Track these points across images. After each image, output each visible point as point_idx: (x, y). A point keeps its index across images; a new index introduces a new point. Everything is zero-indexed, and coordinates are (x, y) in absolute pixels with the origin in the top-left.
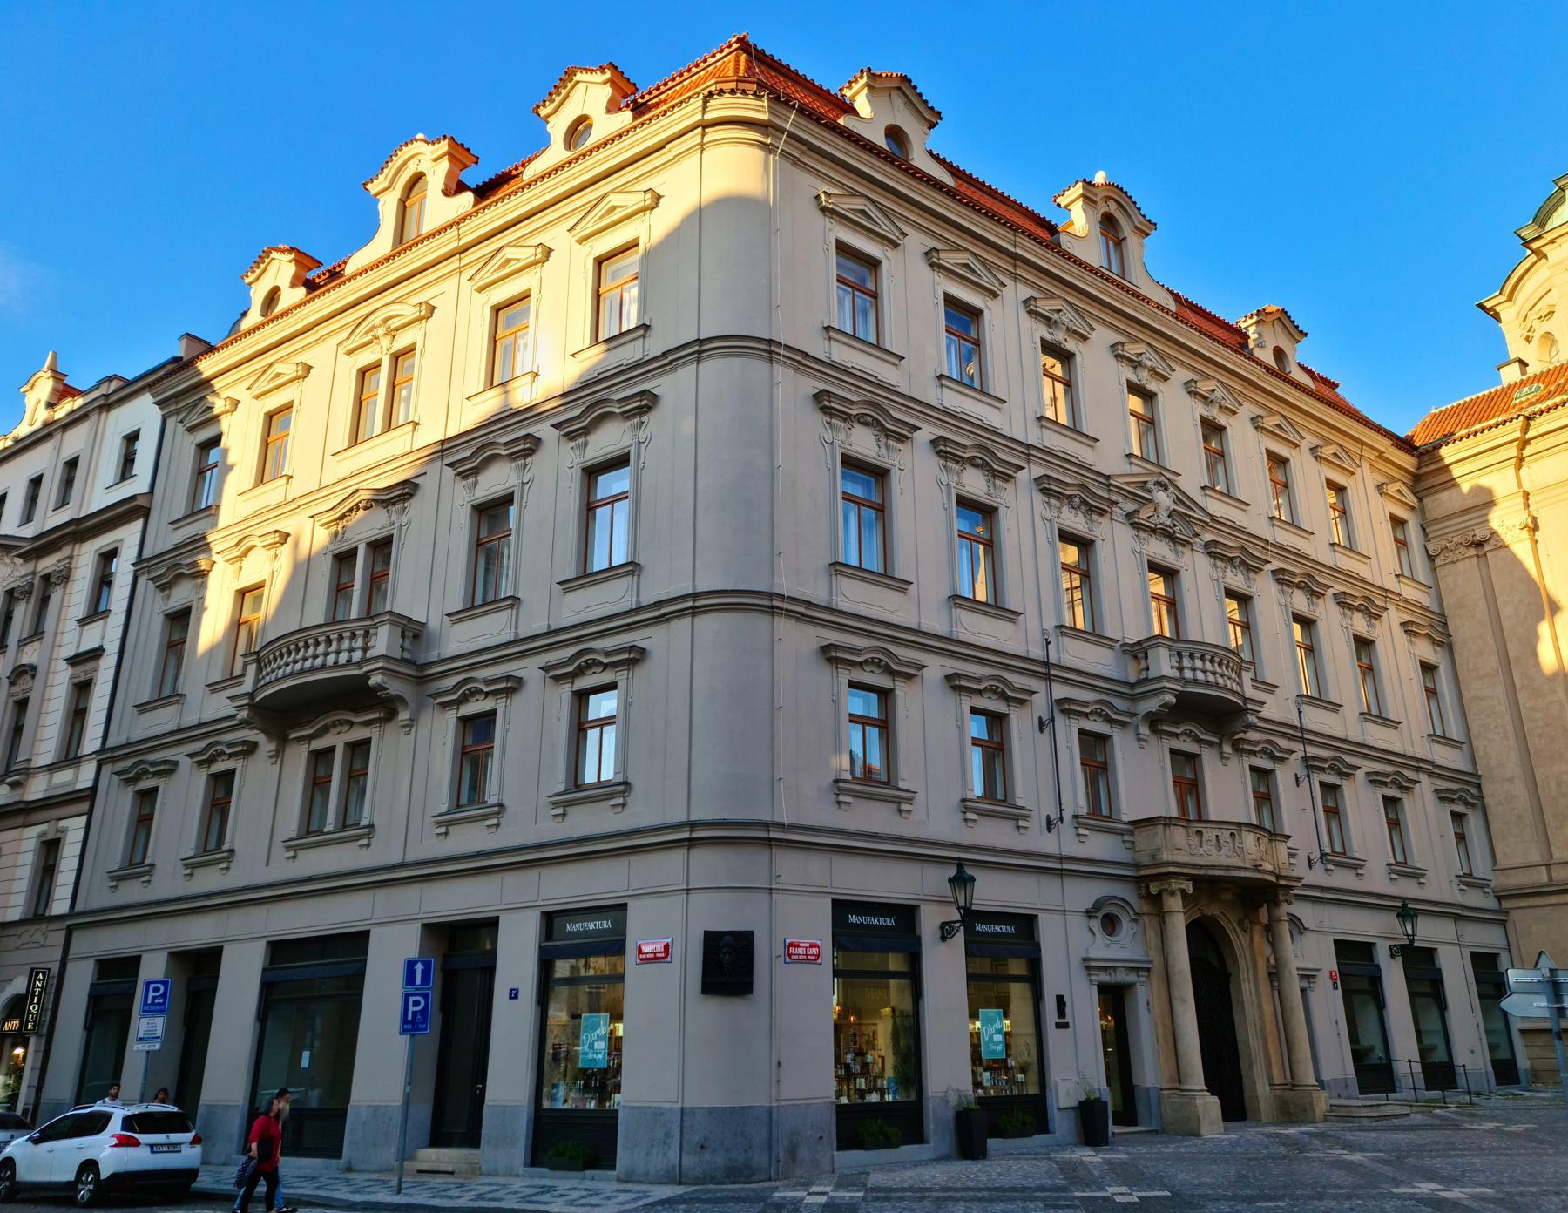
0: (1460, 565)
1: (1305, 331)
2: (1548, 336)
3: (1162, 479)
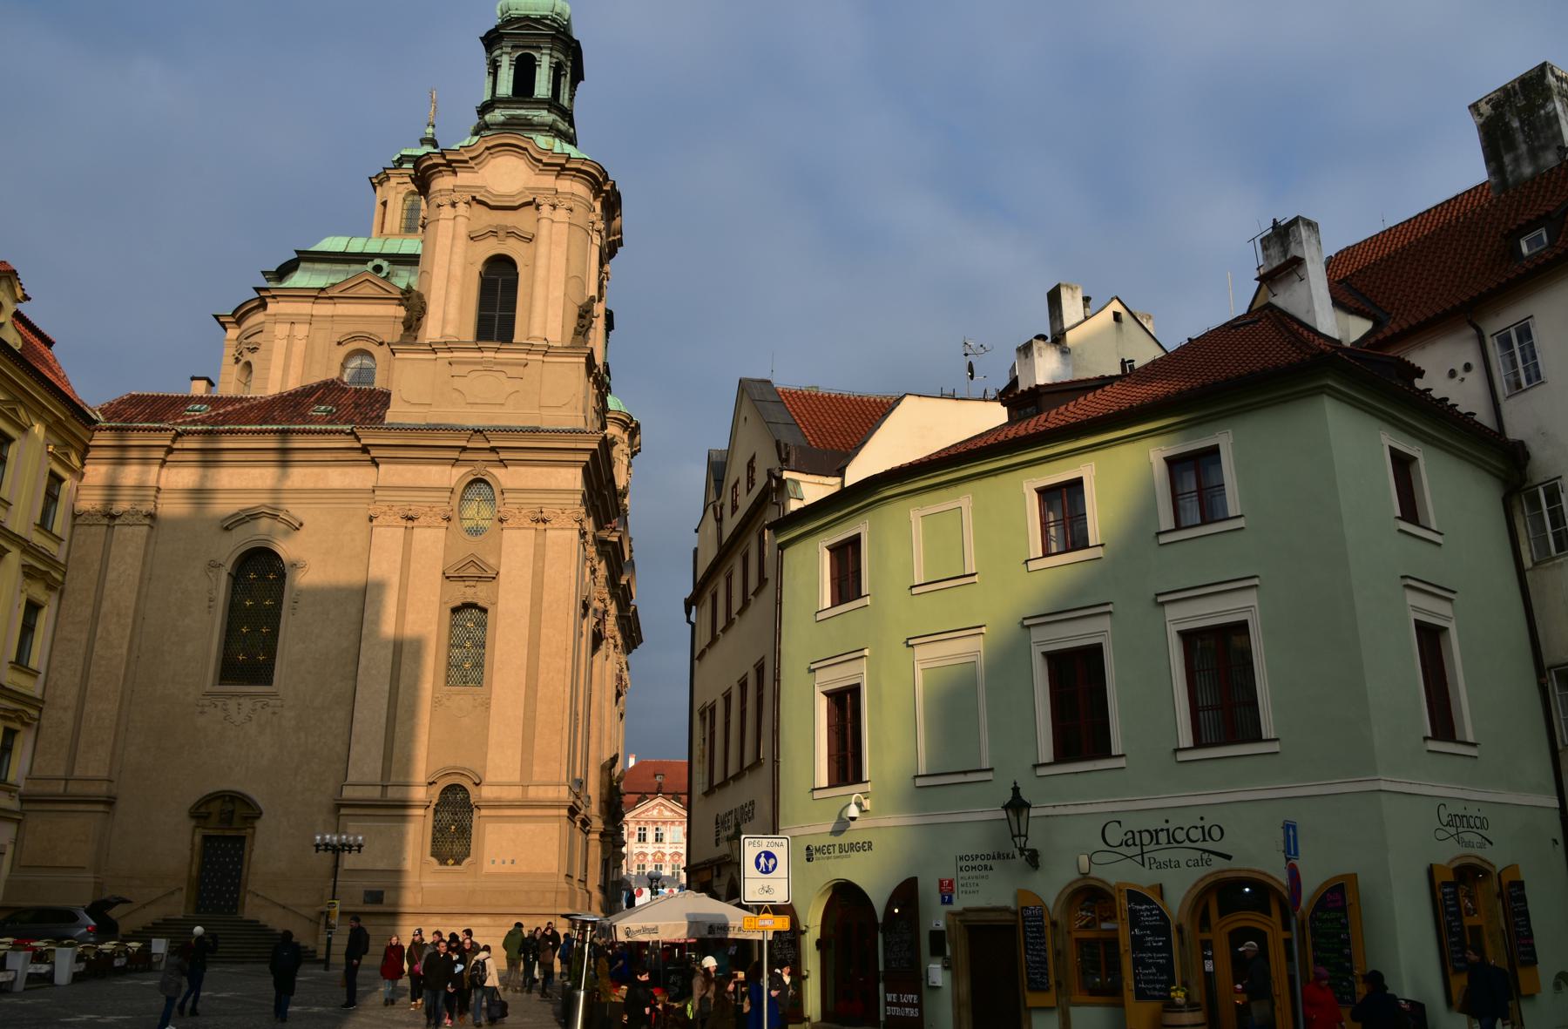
0: (93, 529)
1: (29, 296)
2: (248, 364)
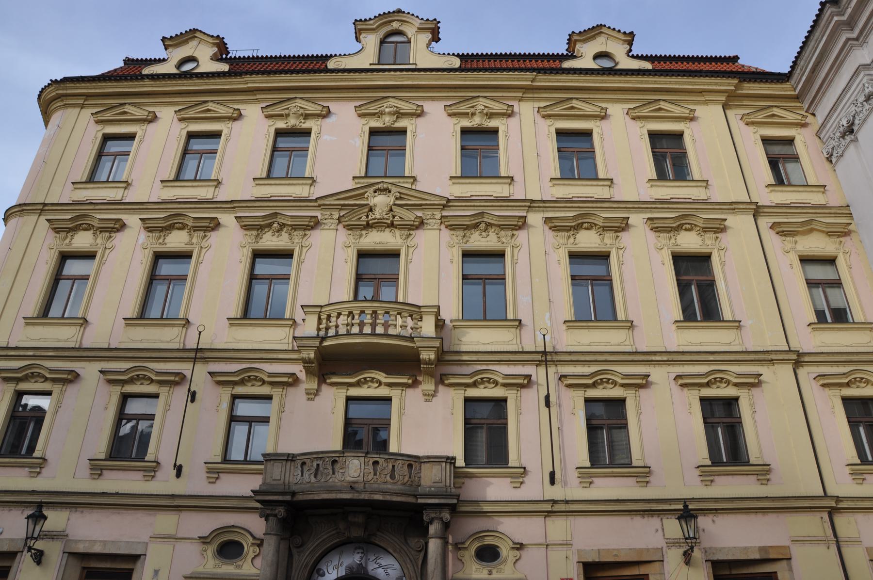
3: (380, 186)
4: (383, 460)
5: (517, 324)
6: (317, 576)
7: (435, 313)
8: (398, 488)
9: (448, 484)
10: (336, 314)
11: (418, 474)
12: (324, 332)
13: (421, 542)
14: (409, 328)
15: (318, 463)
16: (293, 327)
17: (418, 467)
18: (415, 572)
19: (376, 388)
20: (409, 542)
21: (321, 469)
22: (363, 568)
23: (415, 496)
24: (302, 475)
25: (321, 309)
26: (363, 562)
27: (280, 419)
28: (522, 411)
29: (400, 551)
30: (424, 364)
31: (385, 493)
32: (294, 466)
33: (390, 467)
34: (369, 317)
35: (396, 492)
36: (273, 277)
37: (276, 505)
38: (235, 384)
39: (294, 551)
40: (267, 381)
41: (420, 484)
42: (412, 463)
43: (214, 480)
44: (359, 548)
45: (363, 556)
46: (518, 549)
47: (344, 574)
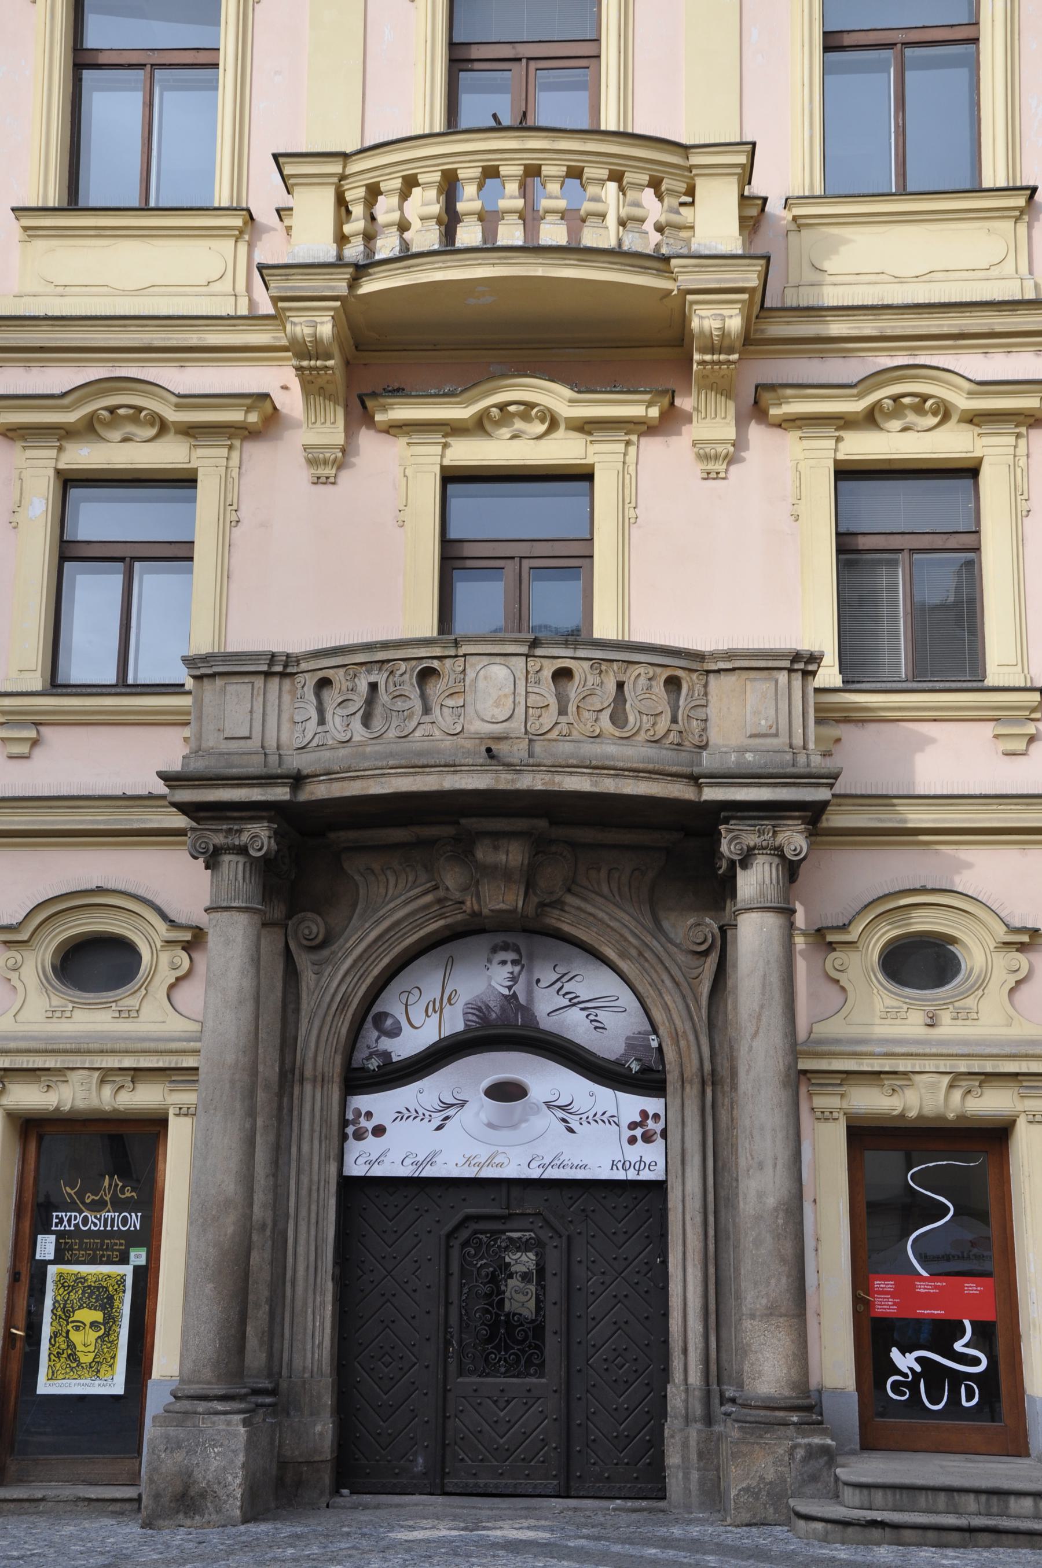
4: (586, 665)
5: (1021, 202)
6: (376, 1034)
7: (739, 170)
8: (636, 753)
9: (798, 741)
10: (397, 183)
11: (700, 709)
12: (362, 248)
13: (708, 925)
14: (649, 226)
15: (372, 679)
16: (247, 237)
17: (698, 689)
18: (691, 1019)
19: (539, 438)
20: (666, 925)
21: (383, 697)
22: (520, 1007)
23: (694, 779)
24: (322, 721)
25: (344, 167)
26: (520, 989)
27: (226, 547)
28: (1033, 504)
29: (640, 954)
30: (703, 351)
31: (598, 768)
32: (293, 692)
33: (611, 687)
34: (512, 187)
35: (635, 765)
36: (157, 59)
37: (241, 819)
38: (65, 434)
39: (304, 961)
40: (173, 423)
41: (707, 744)
42: (680, 673)
43: (24, 749)
44: (505, 948)
45: (520, 973)
46: (1022, 947)
47: (460, 1027)
